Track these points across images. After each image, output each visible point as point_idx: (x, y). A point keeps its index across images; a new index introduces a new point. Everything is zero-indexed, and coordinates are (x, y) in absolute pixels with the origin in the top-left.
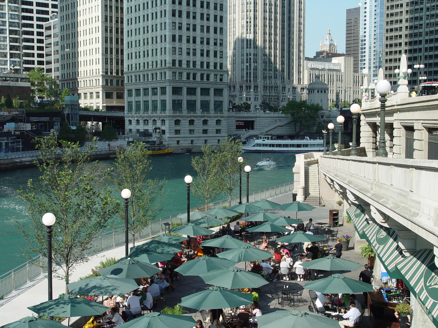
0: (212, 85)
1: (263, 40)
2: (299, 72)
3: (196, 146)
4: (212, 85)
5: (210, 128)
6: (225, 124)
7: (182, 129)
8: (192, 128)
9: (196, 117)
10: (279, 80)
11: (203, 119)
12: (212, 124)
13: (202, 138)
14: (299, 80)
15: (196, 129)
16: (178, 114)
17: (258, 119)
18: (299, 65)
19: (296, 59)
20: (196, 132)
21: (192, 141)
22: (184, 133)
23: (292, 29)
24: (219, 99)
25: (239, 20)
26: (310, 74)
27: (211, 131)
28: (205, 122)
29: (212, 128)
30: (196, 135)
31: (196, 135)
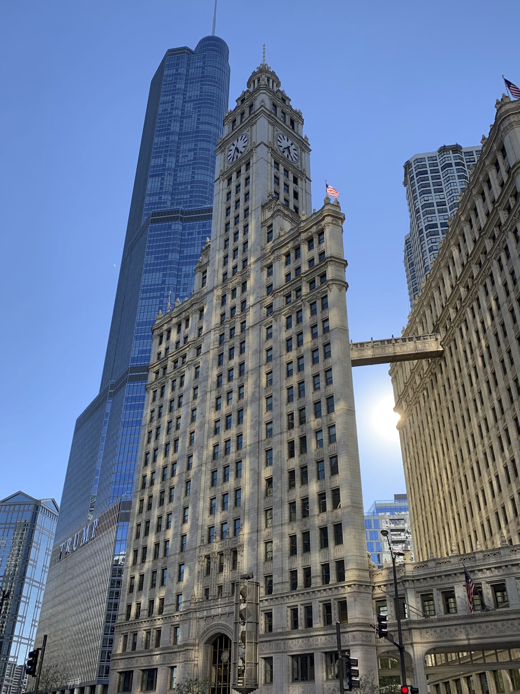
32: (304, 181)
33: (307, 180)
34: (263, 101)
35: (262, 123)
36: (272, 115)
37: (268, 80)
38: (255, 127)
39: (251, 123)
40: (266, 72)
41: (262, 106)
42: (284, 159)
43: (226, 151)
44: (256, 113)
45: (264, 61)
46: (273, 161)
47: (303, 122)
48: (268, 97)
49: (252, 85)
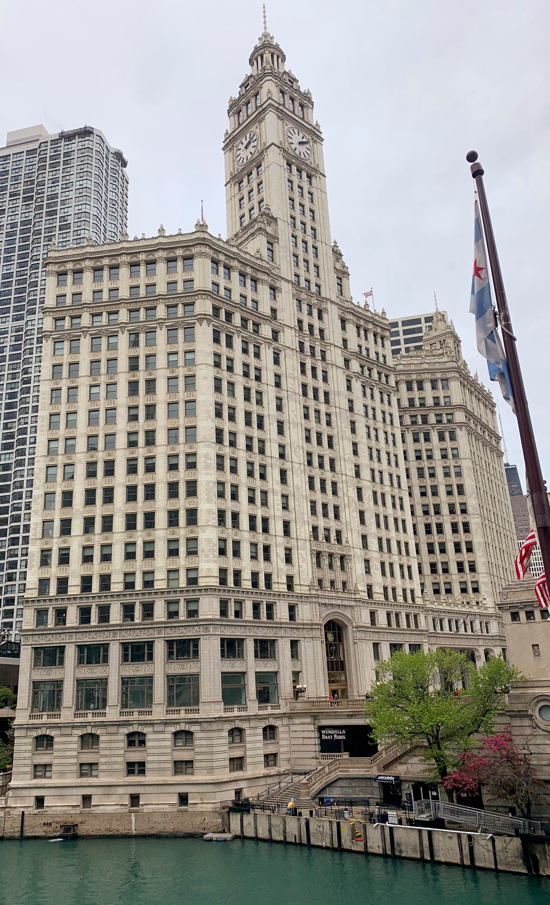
0: (160, 632)
3: (96, 816)
4: (160, 632)
5: (150, 758)
9: (103, 725)
13: (121, 790)
20: (104, 771)
21: (87, 799)
27: (156, 766)
29: (155, 758)
30: (103, 779)
32: (318, 178)
33: (321, 176)
34: (269, 92)
35: (271, 117)
36: (281, 107)
37: (272, 57)
38: (263, 123)
39: (259, 118)
40: (270, 47)
41: (270, 98)
42: (297, 158)
43: (235, 149)
44: (264, 107)
45: (265, 28)
46: (285, 162)
47: (313, 105)
48: (274, 84)
49: (255, 62)
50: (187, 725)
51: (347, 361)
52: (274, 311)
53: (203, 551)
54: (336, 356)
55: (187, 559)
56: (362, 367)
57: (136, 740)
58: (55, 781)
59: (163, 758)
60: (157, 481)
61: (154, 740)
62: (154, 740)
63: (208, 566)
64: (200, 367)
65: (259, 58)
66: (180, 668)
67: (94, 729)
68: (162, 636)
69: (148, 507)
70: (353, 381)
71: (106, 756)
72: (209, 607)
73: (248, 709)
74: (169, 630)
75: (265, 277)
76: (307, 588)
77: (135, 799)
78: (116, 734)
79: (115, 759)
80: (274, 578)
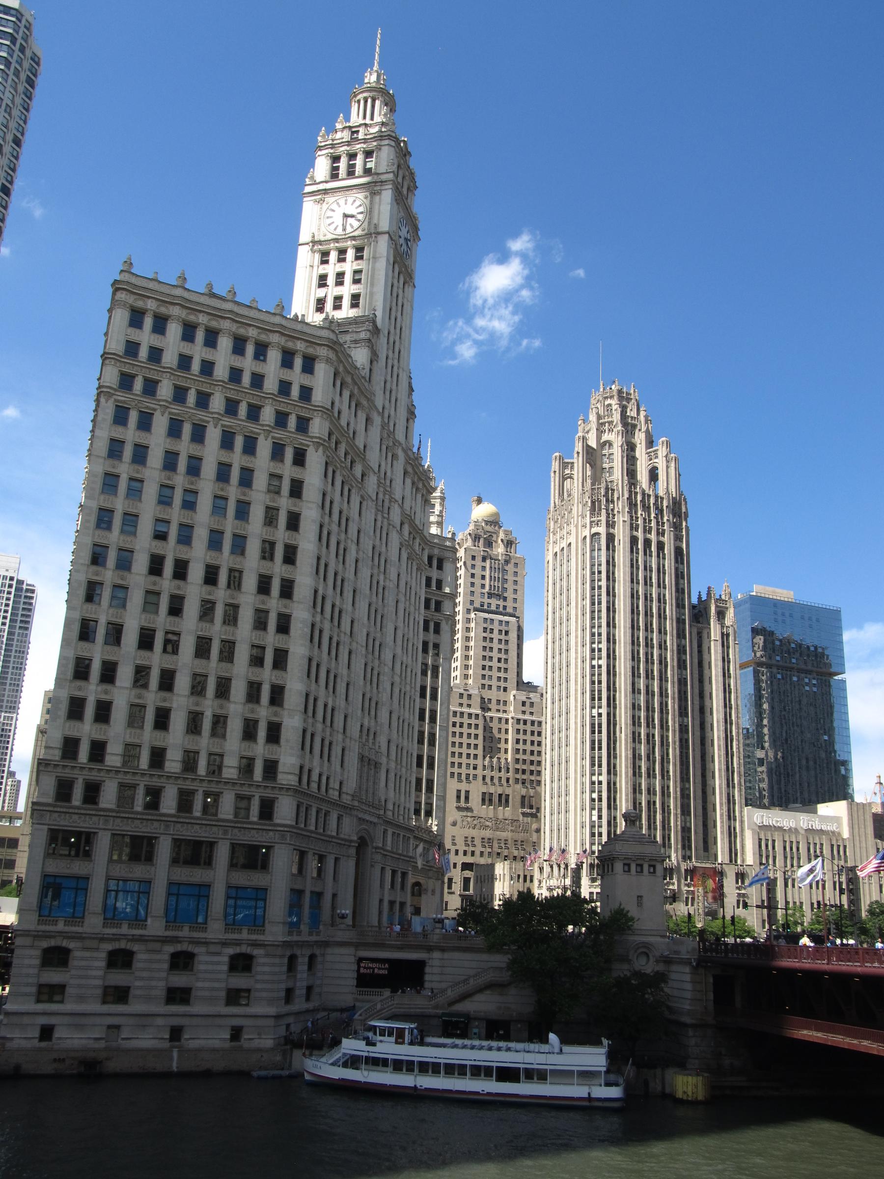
0: (225, 832)
1: (630, 756)
2: (731, 834)
4: (225, 832)
5: (200, 984)
6: (267, 969)
7: (72, 982)
8: (118, 978)
9: (141, 939)
10: (676, 851)
11: (170, 949)
12: (210, 967)
13: (160, 1021)
14: (733, 854)
15: (138, 983)
16: (61, 926)
17: (436, 955)
18: (731, 816)
19: (721, 804)
22: (81, 999)
23: (708, 734)
24: (256, 879)
25: (576, 710)
26: (760, 840)
28: (182, 961)
29: (207, 984)
31: (135, 1007)
38: (377, 198)
43: (325, 206)
49: (362, 103)
50: (249, 948)
51: (402, 524)
52: (365, 447)
53: (287, 741)
54: (396, 516)
55: (267, 747)
56: (410, 533)
57: (182, 961)
58: (69, 1006)
59: (216, 985)
60: (239, 639)
61: (207, 963)
62: (207, 963)
63: (288, 759)
64: (310, 505)
65: (369, 101)
66: (242, 878)
67: (129, 943)
68: (229, 837)
69: (224, 669)
70: (403, 549)
71: (142, 979)
72: (285, 810)
73: (266, 932)
74: (236, 830)
75: (365, 403)
76: (349, 798)
77: (176, 1033)
78: (159, 952)
79: (154, 983)
80: (331, 780)
